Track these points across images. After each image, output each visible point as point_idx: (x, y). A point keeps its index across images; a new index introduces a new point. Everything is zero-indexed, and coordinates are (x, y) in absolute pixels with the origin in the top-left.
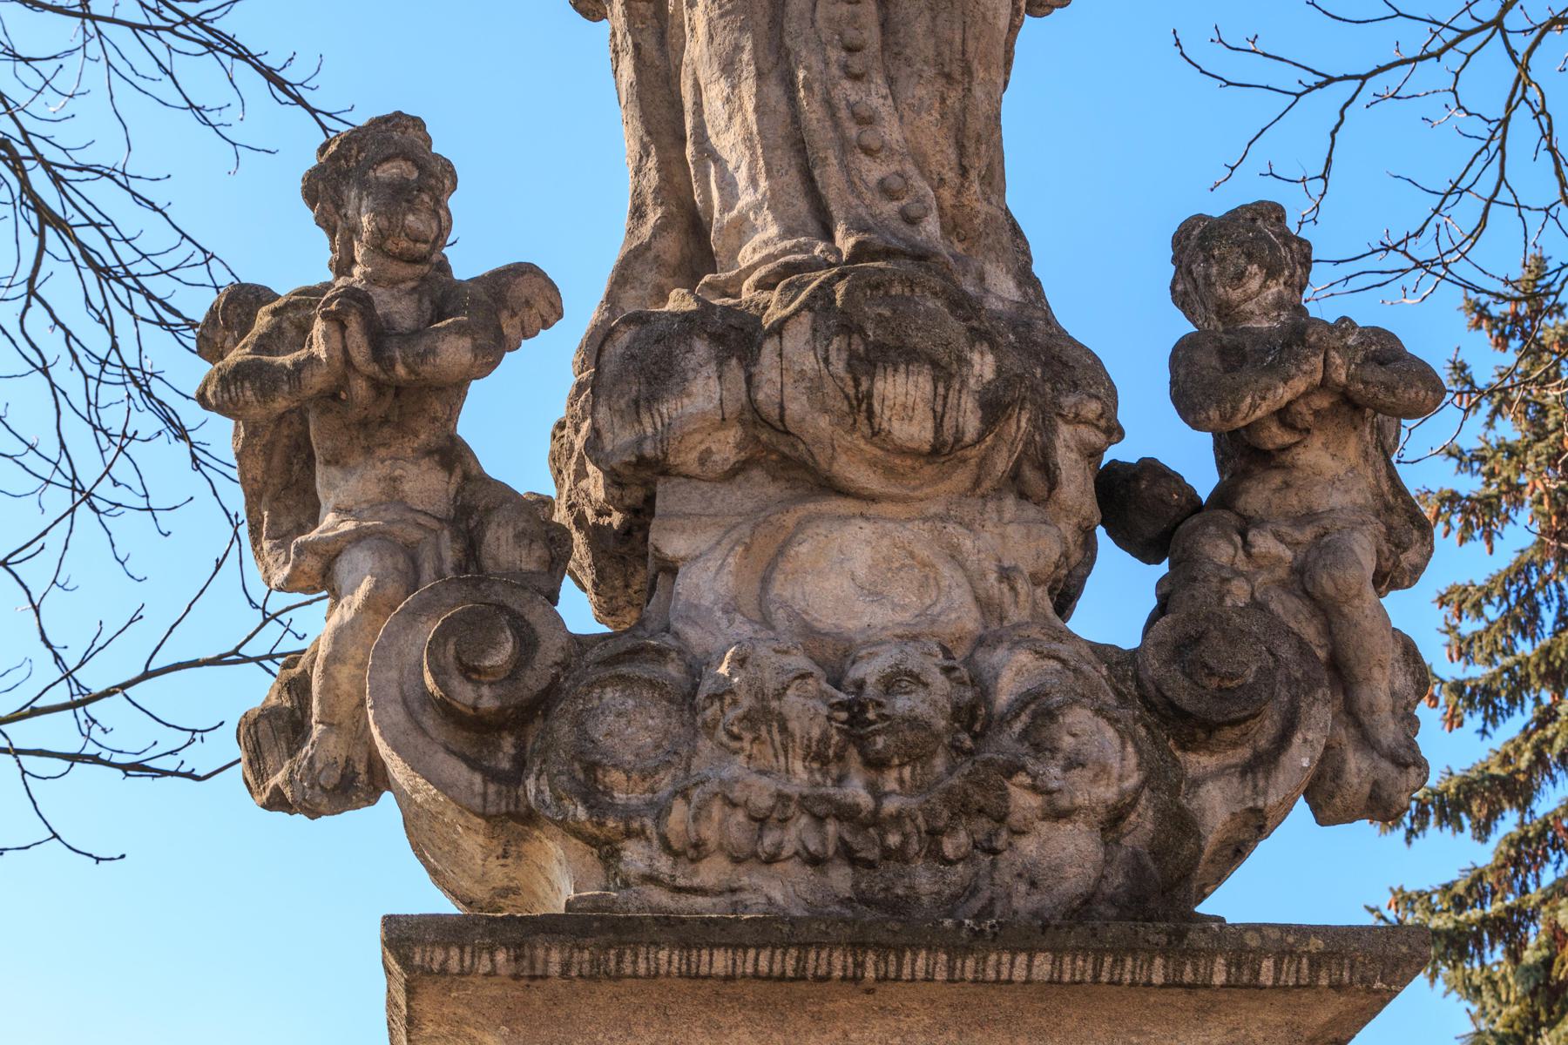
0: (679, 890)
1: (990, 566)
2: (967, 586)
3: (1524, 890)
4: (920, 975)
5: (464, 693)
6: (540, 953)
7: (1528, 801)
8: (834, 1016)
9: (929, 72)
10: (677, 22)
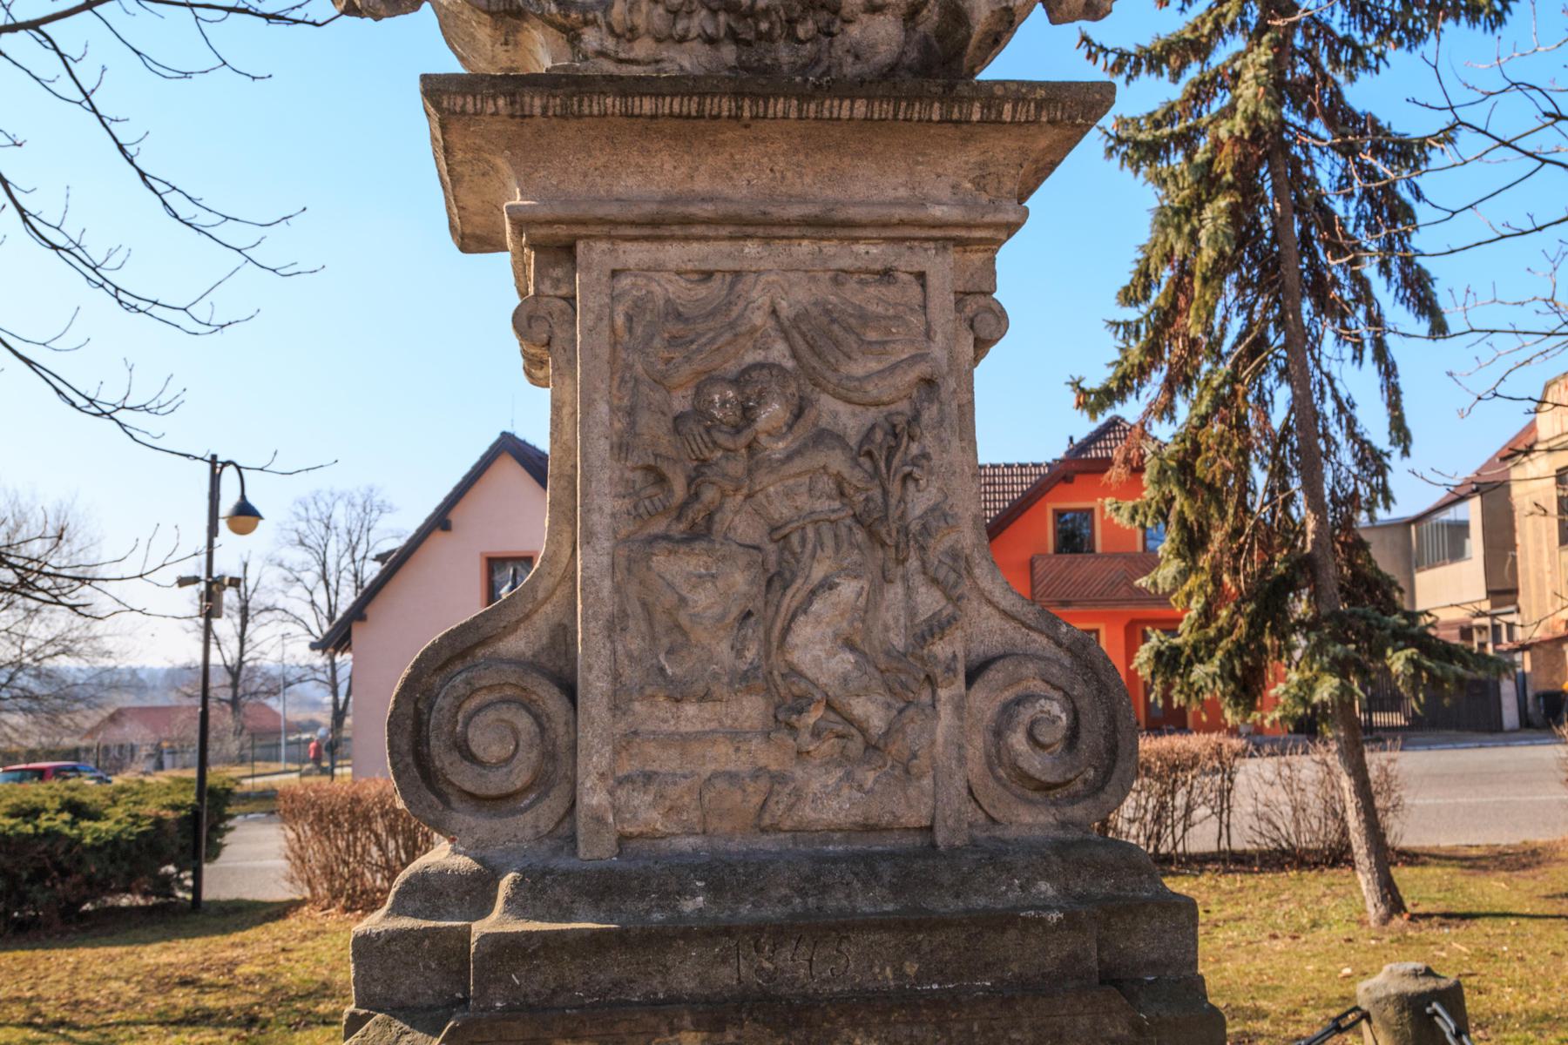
0: (621, 61)
3: (1200, 115)
4: (780, 114)
6: (527, 99)
7: (1206, 57)
8: (724, 143)
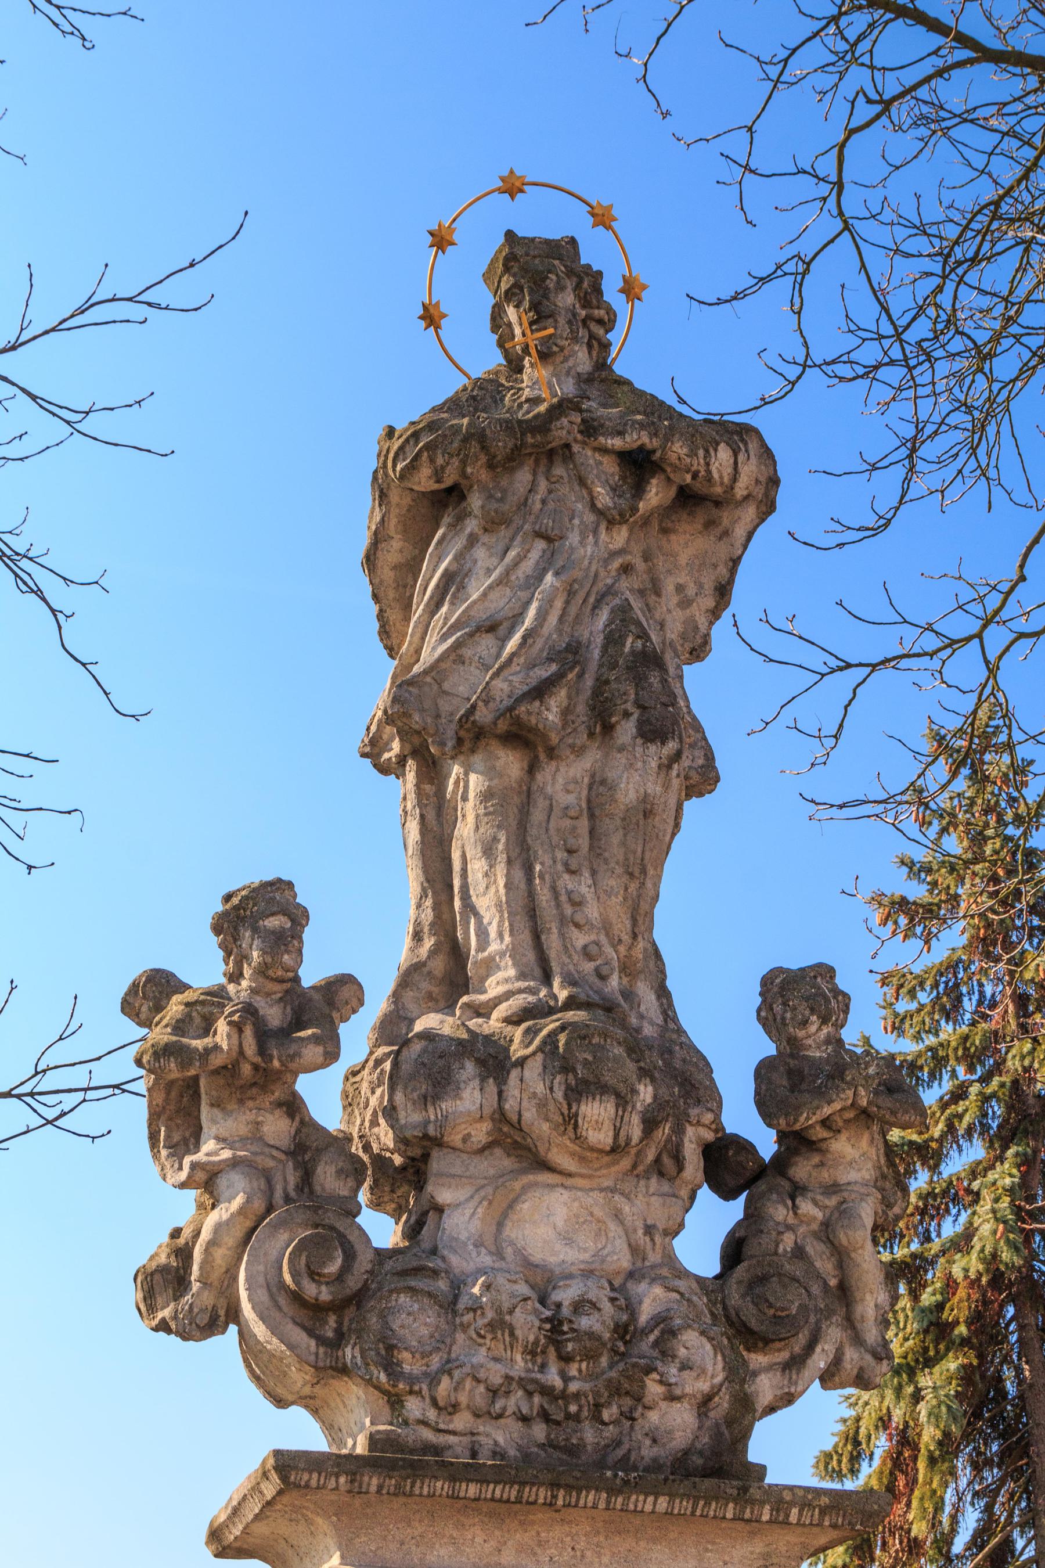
0: (440, 1431)
1: (640, 1224)
2: (624, 1238)
3: (928, 1239)
4: (590, 1504)
5: (310, 1290)
6: (366, 1479)
7: (937, 1165)
8: (533, 1523)
9: (619, 870)
10: (452, 805)
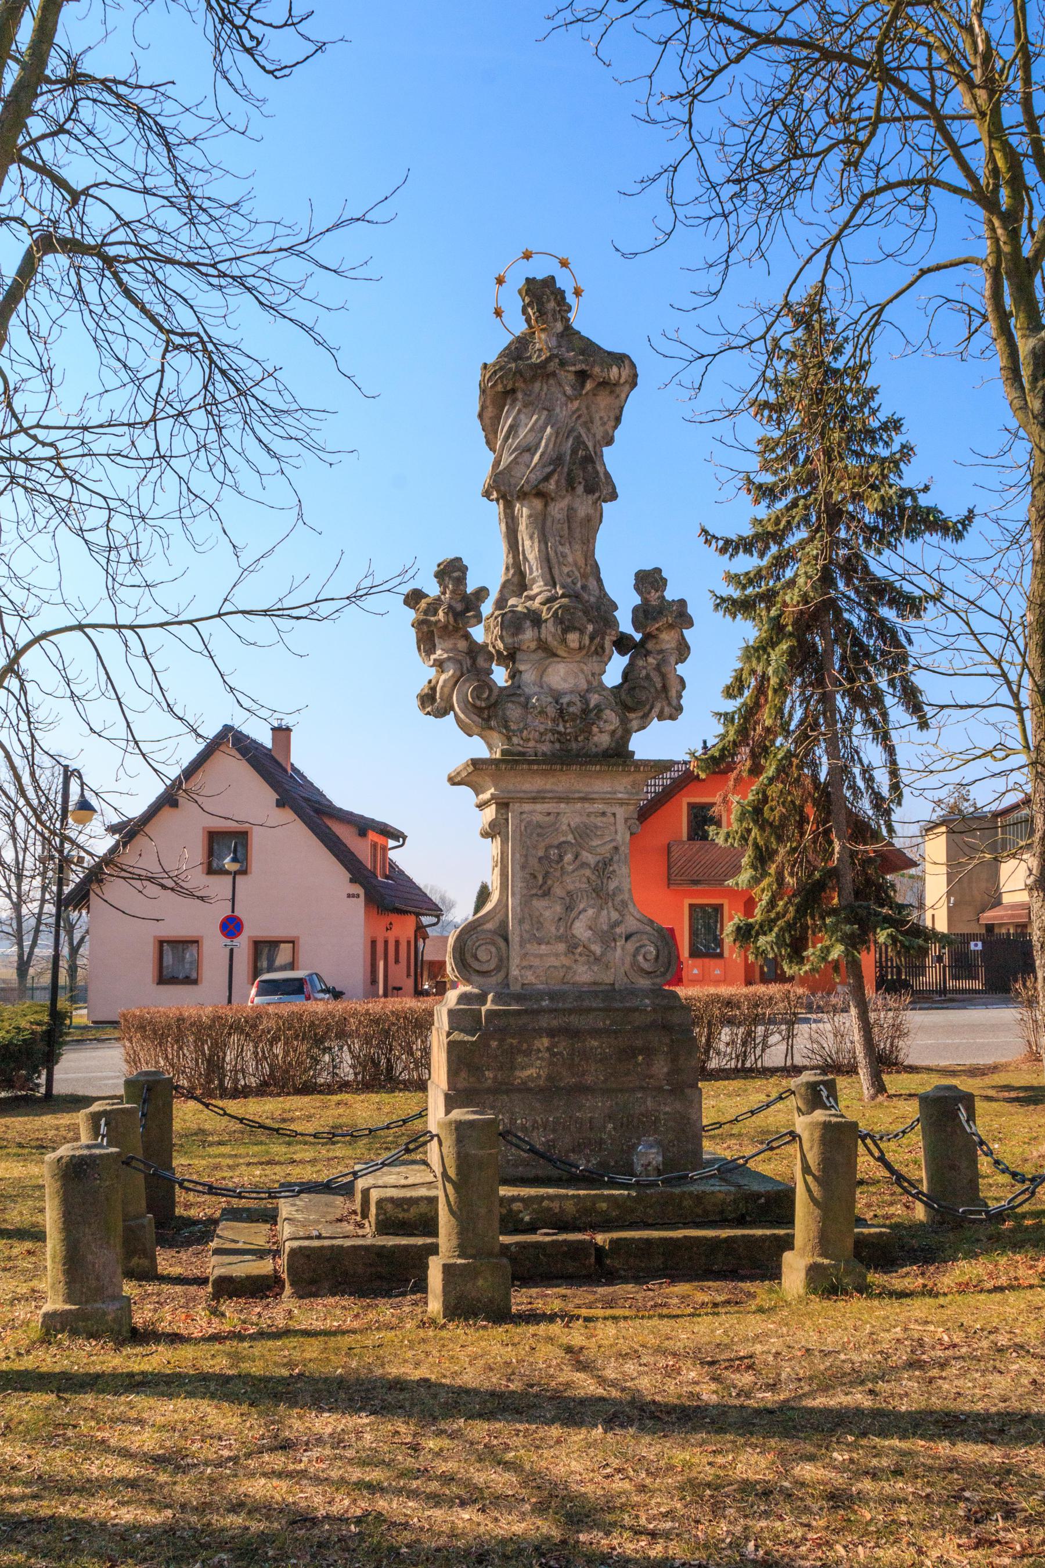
3: (779, 579)
5: (478, 703)
